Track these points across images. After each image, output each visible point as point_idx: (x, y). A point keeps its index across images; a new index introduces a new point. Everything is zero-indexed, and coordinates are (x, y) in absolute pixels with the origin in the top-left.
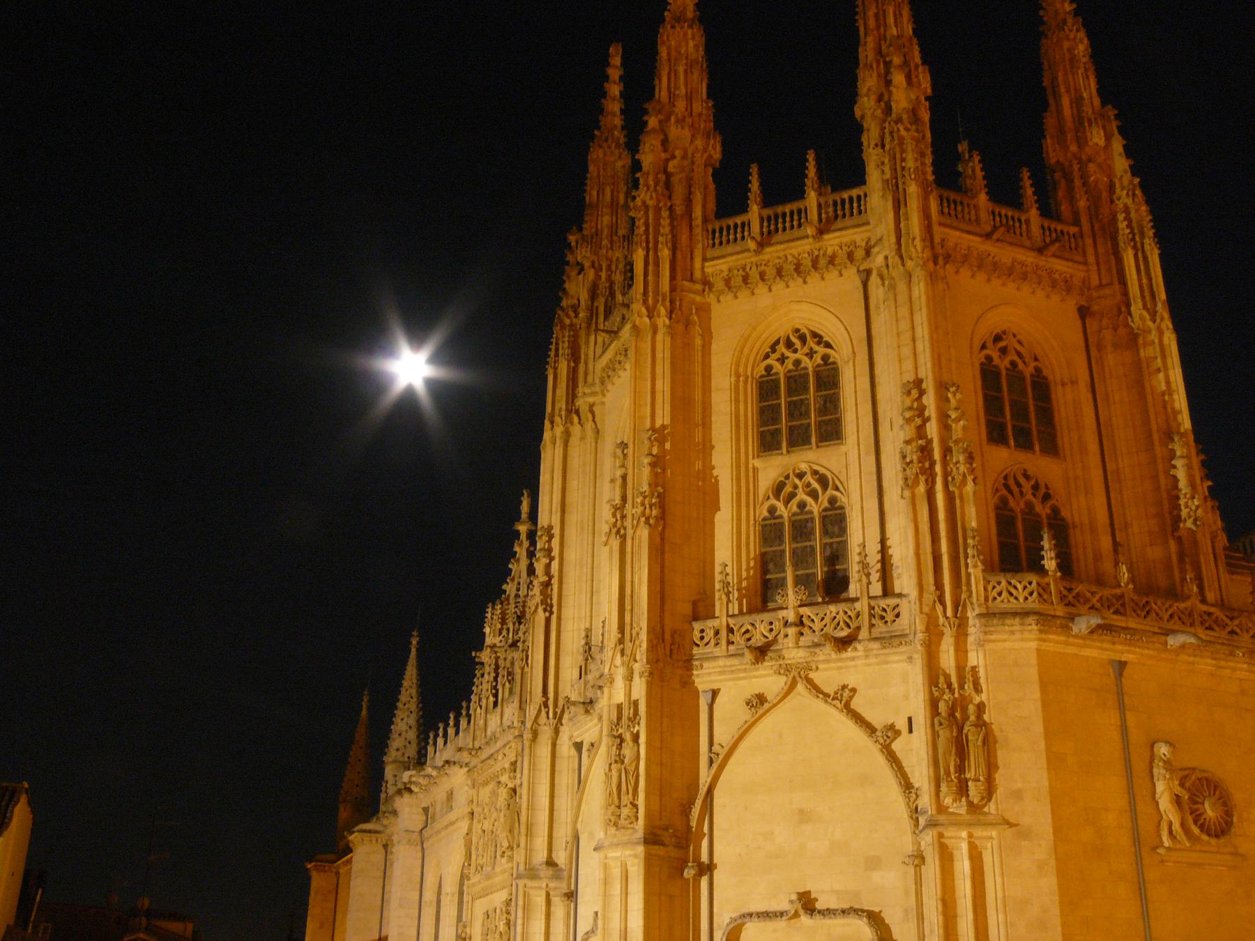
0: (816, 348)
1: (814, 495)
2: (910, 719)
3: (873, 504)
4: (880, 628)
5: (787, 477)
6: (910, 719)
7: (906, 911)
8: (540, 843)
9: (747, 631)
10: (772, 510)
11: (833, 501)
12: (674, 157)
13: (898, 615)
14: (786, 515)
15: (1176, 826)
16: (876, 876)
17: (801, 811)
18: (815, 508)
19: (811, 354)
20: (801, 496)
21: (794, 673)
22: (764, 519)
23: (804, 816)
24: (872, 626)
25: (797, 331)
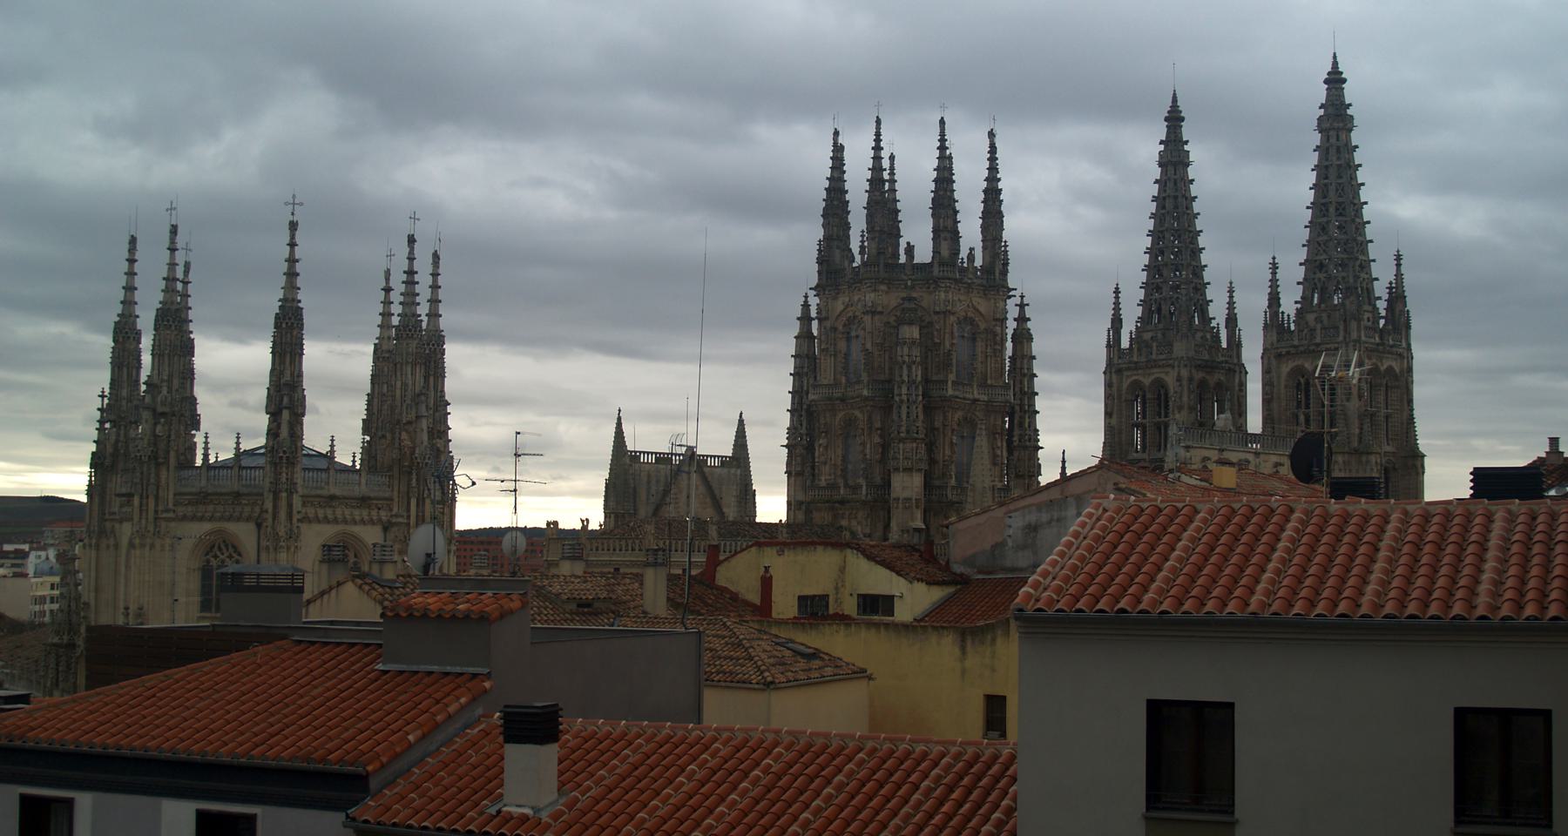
0: (234, 555)
25: (224, 541)
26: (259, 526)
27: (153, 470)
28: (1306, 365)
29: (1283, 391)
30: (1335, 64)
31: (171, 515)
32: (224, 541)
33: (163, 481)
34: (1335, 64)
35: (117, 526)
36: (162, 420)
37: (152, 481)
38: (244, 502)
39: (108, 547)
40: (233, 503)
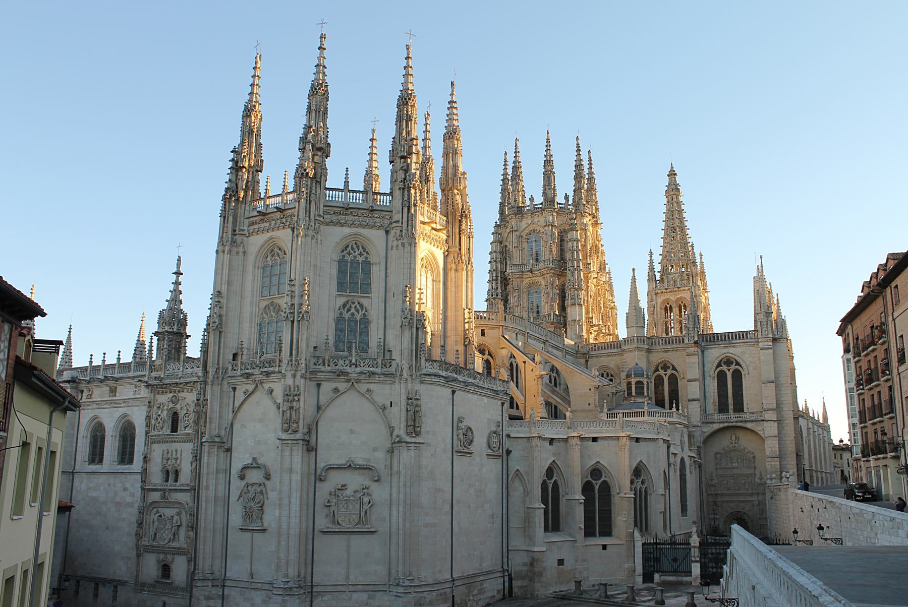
0: (363, 253)
1: (357, 311)
2: (391, 402)
4: (385, 370)
5: (348, 303)
6: (391, 402)
7: (385, 466)
8: (215, 425)
9: (335, 362)
10: (341, 314)
11: (364, 315)
12: (317, 155)
13: (391, 366)
14: (347, 318)
15: (462, 443)
17: (351, 430)
18: (358, 317)
19: (361, 254)
20: (353, 310)
21: (353, 381)
23: (352, 432)
26: (387, 232)
27: (314, 188)
28: (671, 298)
29: (659, 310)
30: (672, 167)
31: (321, 219)
32: (356, 244)
33: (318, 195)
34: (672, 167)
35: (245, 239)
36: (319, 153)
37: (314, 192)
38: (376, 216)
39: (238, 253)
40: (368, 216)
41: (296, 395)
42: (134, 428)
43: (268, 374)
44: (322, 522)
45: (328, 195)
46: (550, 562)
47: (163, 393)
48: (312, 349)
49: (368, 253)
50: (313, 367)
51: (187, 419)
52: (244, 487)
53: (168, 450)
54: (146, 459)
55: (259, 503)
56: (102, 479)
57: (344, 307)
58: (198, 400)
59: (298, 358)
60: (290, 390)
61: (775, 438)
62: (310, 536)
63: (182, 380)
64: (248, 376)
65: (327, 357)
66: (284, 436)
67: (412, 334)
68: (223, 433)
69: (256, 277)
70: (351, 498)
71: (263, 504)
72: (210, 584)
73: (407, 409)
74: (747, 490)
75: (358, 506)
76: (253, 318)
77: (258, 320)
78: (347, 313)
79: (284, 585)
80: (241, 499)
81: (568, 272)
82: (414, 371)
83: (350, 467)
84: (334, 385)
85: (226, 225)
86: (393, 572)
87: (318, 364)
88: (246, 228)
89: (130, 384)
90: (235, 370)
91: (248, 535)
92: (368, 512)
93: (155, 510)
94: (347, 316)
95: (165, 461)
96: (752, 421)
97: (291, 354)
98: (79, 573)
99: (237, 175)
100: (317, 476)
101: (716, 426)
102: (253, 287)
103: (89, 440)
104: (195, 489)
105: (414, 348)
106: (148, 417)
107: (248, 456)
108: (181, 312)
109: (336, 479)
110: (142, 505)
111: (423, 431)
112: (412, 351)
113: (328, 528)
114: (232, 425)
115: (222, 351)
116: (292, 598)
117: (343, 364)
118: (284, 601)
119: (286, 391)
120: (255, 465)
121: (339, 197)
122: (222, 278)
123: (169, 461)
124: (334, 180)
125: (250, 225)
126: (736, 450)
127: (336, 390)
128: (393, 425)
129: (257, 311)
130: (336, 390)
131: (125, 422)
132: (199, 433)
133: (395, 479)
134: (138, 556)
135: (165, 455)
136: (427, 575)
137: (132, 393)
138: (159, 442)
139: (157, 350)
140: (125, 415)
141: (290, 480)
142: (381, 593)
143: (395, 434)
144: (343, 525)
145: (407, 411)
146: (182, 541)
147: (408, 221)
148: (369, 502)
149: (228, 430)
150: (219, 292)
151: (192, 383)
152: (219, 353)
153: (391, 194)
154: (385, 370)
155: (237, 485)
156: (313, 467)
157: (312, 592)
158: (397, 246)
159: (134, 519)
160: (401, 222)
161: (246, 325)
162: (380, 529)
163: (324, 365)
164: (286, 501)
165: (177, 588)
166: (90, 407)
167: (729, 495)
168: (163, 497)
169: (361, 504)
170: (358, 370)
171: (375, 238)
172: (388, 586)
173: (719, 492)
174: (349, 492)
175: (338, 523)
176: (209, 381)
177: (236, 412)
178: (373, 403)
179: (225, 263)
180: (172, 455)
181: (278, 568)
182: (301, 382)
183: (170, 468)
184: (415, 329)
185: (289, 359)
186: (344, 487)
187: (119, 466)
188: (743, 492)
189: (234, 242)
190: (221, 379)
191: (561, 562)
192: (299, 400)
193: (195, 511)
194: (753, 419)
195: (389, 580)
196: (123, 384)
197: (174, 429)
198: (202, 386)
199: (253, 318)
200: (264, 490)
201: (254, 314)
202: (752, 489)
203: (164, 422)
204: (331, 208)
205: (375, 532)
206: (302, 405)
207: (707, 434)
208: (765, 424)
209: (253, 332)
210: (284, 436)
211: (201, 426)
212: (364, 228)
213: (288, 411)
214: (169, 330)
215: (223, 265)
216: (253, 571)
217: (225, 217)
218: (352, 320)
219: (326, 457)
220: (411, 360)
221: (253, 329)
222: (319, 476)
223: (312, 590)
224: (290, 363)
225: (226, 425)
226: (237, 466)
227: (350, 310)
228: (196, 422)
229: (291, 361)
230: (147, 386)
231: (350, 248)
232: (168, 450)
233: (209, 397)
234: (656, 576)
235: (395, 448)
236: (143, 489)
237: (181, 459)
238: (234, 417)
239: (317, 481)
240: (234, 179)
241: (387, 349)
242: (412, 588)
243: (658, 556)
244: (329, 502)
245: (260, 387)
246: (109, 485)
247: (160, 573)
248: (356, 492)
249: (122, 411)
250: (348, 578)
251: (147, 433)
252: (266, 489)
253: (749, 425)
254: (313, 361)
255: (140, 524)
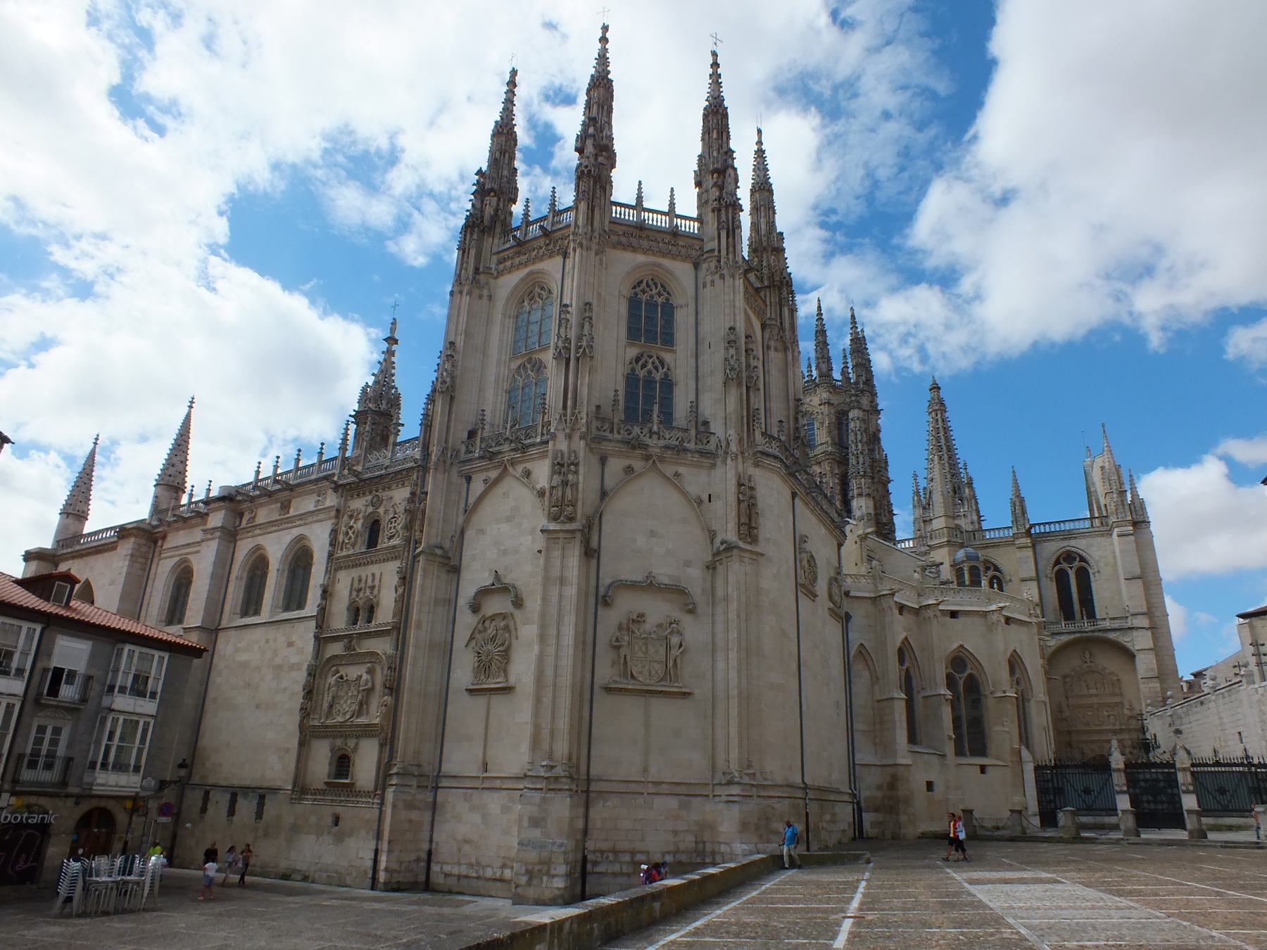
1: (656, 368)
3: (692, 383)
5: (642, 356)
7: (703, 590)
9: (628, 430)
10: (633, 370)
11: (666, 375)
13: (708, 442)
16: (689, 570)
17: (652, 531)
18: (658, 376)
19: (659, 294)
20: (650, 366)
21: (655, 458)
22: (628, 374)
23: (653, 534)
24: (696, 444)
26: (696, 266)
32: (652, 280)
35: (492, 281)
38: (681, 243)
39: (480, 297)
41: (572, 464)
42: (311, 557)
43: (524, 449)
44: (606, 672)
45: (614, 211)
46: (918, 779)
47: (358, 495)
48: (594, 408)
49: (668, 293)
50: (594, 432)
51: (393, 525)
52: (478, 623)
53: (360, 576)
54: (326, 593)
55: (503, 645)
56: (258, 634)
57: (637, 361)
58: (413, 494)
59: (576, 411)
60: (562, 459)
61: (1150, 652)
62: (587, 696)
63: (391, 470)
64: (493, 456)
65: (616, 420)
66: (552, 526)
67: (741, 394)
68: (447, 545)
69: (506, 330)
70: (653, 636)
71: (509, 648)
72: (414, 783)
73: (738, 497)
74: (1114, 725)
75: (662, 651)
76: (501, 382)
77: (506, 386)
78: (642, 369)
79: (545, 772)
80: (473, 643)
81: (850, 456)
82: (745, 446)
83: (649, 586)
84: (627, 462)
85: (465, 260)
86: (720, 762)
87: (602, 430)
88: (493, 266)
89: (312, 492)
90: (471, 452)
91: (481, 701)
92: (678, 661)
93: (334, 668)
94: (642, 373)
95: (354, 593)
96: (1114, 630)
97: (565, 407)
98: (211, 781)
99: (482, 202)
100: (600, 599)
101: (1065, 638)
102: (501, 340)
103: (243, 583)
104: (399, 629)
105: (745, 414)
106: (334, 532)
107: (487, 574)
108: (394, 387)
109: (627, 604)
110: (312, 663)
111: (761, 537)
112: (742, 417)
113: (615, 682)
114: (462, 532)
115: (452, 424)
116: (559, 795)
117: (639, 433)
118: (544, 800)
119: (556, 459)
120: (499, 587)
121: (631, 216)
122: (456, 327)
123: (361, 594)
124: (622, 189)
125: (500, 263)
126: (1092, 671)
127: (629, 470)
128: (714, 528)
129: (506, 373)
130: (629, 470)
131: (299, 550)
132: (411, 542)
133: (720, 610)
134: (302, 744)
135: (356, 586)
136: (779, 767)
137: (313, 505)
138: (347, 567)
139: (355, 438)
140: (301, 538)
141: (561, 597)
142: (699, 799)
143: (718, 540)
144: (640, 679)
145: (739, 501)
146: (374, 716)
147: (727, 248)
148: (681, 646)
149: (455, 539)
150: (452, 344)
151: (404, 473)
152: (448, 427)
153: (699, 219)
154: (701, 447)
155: (466, 621)
156: (593, 583)
157: (587, 791)
158: (713, 282)
159: (299, 689)
160: (717, 250)
161: (490, 393)
162: (696, 691)
163: (612, 431)
164: (552, 631)
165: (359, 794)
166: (249, 534)
167: (1089, 732)
168: (348, 648)
169: (668, 647)
170: (662, 443)
171: (681, 271)
172: (711, 786)
173: (1074, 728)
174: (649, 625)
175: (632, 676)
176: (432, 465)
177: (470, 511)
178: (683, 493)
179: (462, 308)
180: (366, 583)
181: (535, 743)
182: (579, 446)
183: (361, 603)
184: (745, 388)
185: (561, 411)
186: (640, 619)
187: (284, 614)
188: (1106, 728)
189: (475, 281)
190: (449, 463)
191: (930, 786)
192: (576, 473)
193: (398, 663)
194: (1116, 626)
195: (713, 777)
196: (300, 495)
197: (372, 542)
198: (421, 473)
199: (501, 382)
200: (511, 624)
201: (501, 378)
202: (1121, 724)
203: (357, 536)
204: (619, 227)
205: (689, 694)
206: (581, 478)
207: (1053, 648)
208: (1135, 633)
209: (499, 401)
210: (552, 526)
211: (416, 531)
212: (663, 257)
213: (560, 489)
214: (374, 409)
215: (459, 310)
216: (488, 760)
217: (464, 251)
218: (649, 382)
219: (615, 568)
220: (743, 431)
221: (500, 398)
222: (604, 597)
223: (588, 788)
224: (563, 419)
225: (453, 533)
226: (468, 590)
227: (646, 366)
228: (409, 527)
229: (565, 415)
230: (337, 488)
231: (644, 284)
232: (360, 576)
233: (429, 489)
234: (1062, 818)
235: (718, 564)
236: (317, 638)
237: (379, 587)
238: (467, 521)
239: (599, 607)
240: (478, 205)
241: (701, 419)
242: (754, 789)
243: (1060, 786)
244: (617, 640)
245: (510, 469)
246: (267, 641)
247: (334, 769)
248: (660, 626)
249: (295, 532)
250: (645, 770)
251: (330, 555)
252: (515, 623)
253: (1111, 636)
254: (595, 424)
255: (309, 693)
